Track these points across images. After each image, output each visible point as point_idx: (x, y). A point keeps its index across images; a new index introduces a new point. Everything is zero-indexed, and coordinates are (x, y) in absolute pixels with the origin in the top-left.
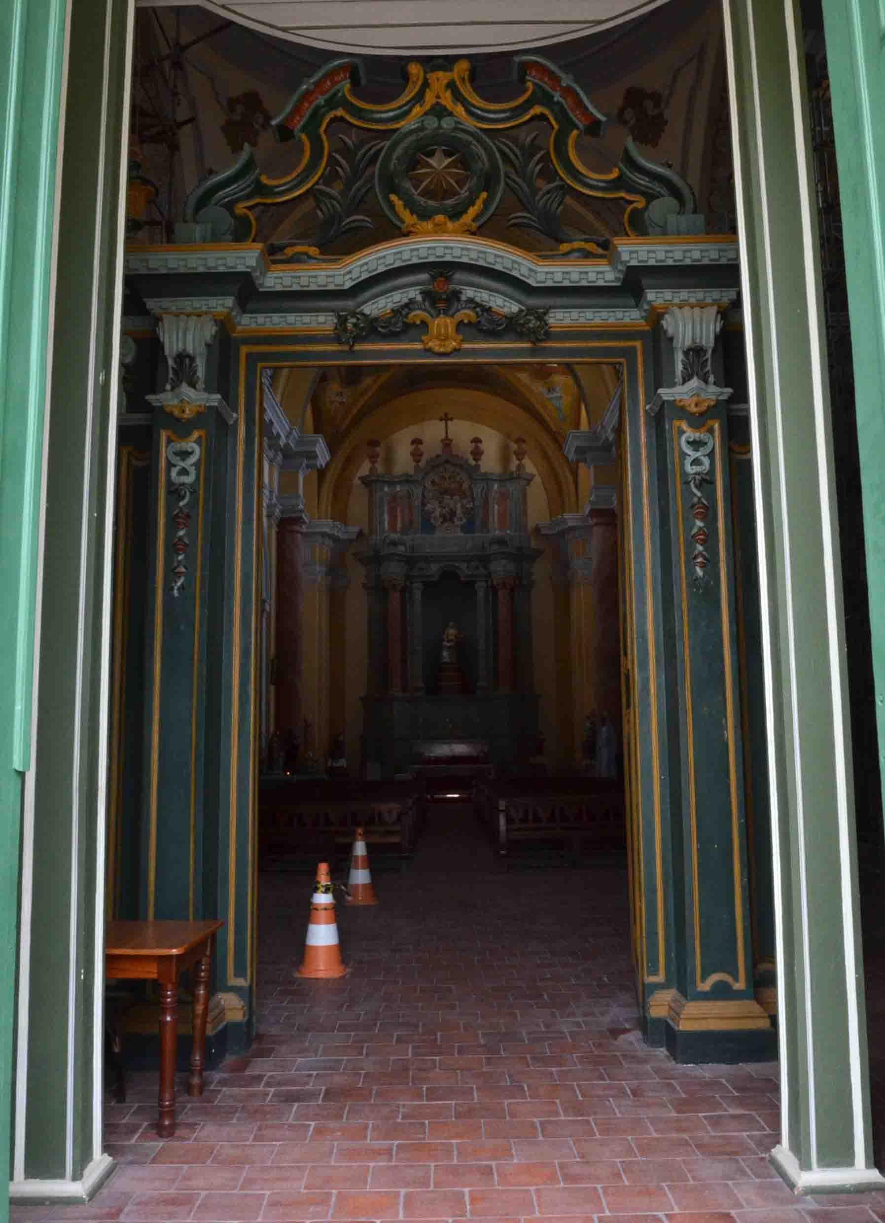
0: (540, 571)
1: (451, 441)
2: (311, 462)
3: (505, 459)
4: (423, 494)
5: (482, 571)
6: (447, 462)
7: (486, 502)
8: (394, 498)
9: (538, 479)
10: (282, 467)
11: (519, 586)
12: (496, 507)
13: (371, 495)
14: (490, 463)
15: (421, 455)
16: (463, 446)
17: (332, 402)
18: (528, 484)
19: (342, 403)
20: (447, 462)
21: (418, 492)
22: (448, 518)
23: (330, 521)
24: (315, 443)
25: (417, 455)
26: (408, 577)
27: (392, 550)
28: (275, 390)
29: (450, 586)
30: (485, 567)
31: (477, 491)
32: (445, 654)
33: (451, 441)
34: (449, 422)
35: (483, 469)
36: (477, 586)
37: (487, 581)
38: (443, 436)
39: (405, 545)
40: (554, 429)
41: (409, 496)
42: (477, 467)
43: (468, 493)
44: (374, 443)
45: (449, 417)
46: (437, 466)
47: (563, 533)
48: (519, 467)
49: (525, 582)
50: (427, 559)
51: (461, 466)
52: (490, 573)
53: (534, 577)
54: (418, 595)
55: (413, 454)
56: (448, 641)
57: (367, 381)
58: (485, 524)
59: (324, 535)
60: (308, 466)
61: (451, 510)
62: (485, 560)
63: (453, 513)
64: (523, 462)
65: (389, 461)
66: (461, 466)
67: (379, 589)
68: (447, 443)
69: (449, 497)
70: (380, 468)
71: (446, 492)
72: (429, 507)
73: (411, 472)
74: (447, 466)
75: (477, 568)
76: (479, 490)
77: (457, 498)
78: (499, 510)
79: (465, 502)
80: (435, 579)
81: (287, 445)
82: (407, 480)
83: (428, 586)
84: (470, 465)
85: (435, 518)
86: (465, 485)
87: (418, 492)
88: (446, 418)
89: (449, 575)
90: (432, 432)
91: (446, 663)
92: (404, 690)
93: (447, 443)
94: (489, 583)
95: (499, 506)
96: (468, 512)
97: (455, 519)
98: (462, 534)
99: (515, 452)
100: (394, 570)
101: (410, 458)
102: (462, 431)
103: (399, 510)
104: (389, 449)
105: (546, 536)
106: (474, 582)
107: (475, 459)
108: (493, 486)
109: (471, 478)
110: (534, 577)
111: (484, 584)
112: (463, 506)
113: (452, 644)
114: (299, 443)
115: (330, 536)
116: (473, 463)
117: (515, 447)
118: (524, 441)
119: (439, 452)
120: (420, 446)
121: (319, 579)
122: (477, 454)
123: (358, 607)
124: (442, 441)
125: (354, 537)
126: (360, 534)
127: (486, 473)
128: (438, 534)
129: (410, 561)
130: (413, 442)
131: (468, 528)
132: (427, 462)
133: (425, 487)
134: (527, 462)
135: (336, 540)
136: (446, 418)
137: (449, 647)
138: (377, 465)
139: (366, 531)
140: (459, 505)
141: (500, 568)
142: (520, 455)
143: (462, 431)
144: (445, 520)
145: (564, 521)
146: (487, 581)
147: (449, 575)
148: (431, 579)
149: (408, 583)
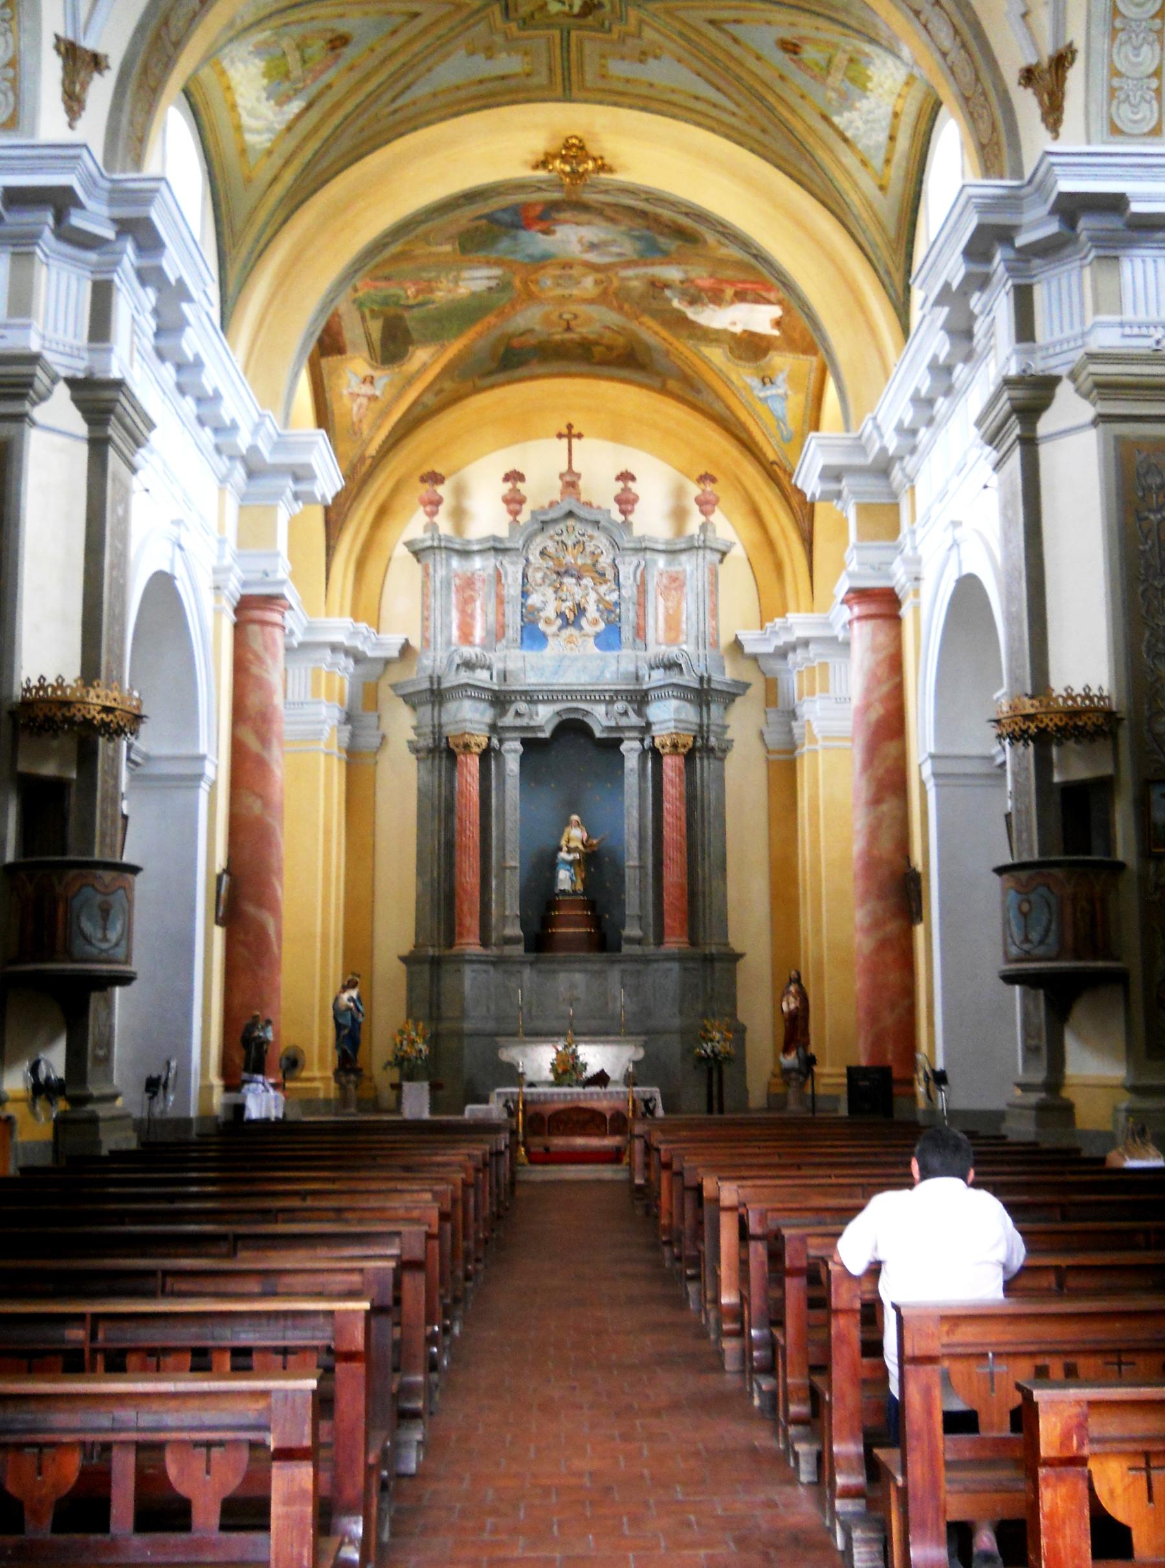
0: (742, 725)
1: (579, 476)
2: (303, 487)
3: (679, 515)
4: (525, 576)
5: (634, 720)
6: (570, 514)
7: (642, 588)
8: (469, 583)
9: (738, 552)
10: (244, 497)
11: (701, 751)
12: (661, 599)
13: (426, 574)
14: (651, 520)
15: (521, 501)
16: (600, 489)
17: (354, 396)
18: (721, 561)
19: (372, 398)
20: (570, 514)
21: (513, 571)
22: (573, 618)
23: (348, 621)
24: (309, 446)
25: (514, 502)
26: (494, 728)
27: (465, 677)
28: (233, 346)
29: (571, 750)
30: (640, 713)
31: (627, 570)
32: (563, 875)
33: (579, 476)
34: (575, 441)
35: (637, 531)
37: (642, 740)
38: (565, 468)
39: (489, 668)
40: (771, 456)
41: (498, 577)
42: (627, 525)
43: (610, 575)
44: (435, 478)
45: (575, 431)
46: (555, 521)
47: (783, 653)
48: (704, 528)
49: (713, 741)
50: (531, 697)
51: (596, 523)
52: (649, 725)
53: (729, 735)
54: (512, 764)
55: (507, 501)
56: (569, 851)
57: (420, 356)
58: (640, 631)
59: (335, 648)
60: (296, 496)
61: (578, 605)
62: (640, 699)
63: (580, 610)
64: (712, 518)
65: (459, 515)
66: (596, 523)
67: (442, 752)
68: (571, 482)
69: (574, 581)
70: (445, 526)
71: (567, 572)
72: (534, 600)
73: (503, 531)
74: (571, 522)
75: (625, 713)
76: (632, 569)
77: (587, 581)
78: (667, 609)
79: (603, 589)
80: (546, 734)
81: (253, 449)
82: (497, 548)
83: (532, 746)
84: (613, 523)
85: (548, 622)
86: (604, 561)
87: (513, 571)
88: (569, 434)
89: (573, 729)
90: (542, 462)
91: (563, 892)
92: (485, 942)
93: (571, 482)
94: (647, 743)
95: (666, 600)
96: (611, 612)
97: (584, 622)
98: (597, 650)
99: (700, 502)
100: (470, 718)
101: (504, 507)
102: (598, 463)
103: (478, 603)
104: (460, 491)
105: (755, 658)
106: (620, 741)
107: (623, 512)
108: (655, 562)
109: (615, 545)
110: (729, 735)
111: (636, 745)
112: (600, 600)
113: (578, 856)
114: (280, 444)
115: (350, 652)
116: (620, 518)
117: (694, 490)
118: (713, 480)
119: (557, 496)
120: (519, 485)
121: (327, 729)
122: (626, 502)
123: (400, 781)
124: (562, 476)
125: (395, 653)
126: (406, 649)
127: (642, 539)
128: (555, 647)
129: (500, 700)
130: (507, 478)
131: (609, 638)
132: (533, 513)
133: (527, 560)
134: (718, 518)
135: (358, 658)
136: (569, 434)
137: (571, 863)
138: (436, 519)
139: (416, 642)
140: (593, 596)
141: (668, 716)
142: (706, 505)
143: (598, 463)
144: (566, 623)
145: (788, 629)
146: (642, 740)
147: (573, 729)
148: (541, 735)
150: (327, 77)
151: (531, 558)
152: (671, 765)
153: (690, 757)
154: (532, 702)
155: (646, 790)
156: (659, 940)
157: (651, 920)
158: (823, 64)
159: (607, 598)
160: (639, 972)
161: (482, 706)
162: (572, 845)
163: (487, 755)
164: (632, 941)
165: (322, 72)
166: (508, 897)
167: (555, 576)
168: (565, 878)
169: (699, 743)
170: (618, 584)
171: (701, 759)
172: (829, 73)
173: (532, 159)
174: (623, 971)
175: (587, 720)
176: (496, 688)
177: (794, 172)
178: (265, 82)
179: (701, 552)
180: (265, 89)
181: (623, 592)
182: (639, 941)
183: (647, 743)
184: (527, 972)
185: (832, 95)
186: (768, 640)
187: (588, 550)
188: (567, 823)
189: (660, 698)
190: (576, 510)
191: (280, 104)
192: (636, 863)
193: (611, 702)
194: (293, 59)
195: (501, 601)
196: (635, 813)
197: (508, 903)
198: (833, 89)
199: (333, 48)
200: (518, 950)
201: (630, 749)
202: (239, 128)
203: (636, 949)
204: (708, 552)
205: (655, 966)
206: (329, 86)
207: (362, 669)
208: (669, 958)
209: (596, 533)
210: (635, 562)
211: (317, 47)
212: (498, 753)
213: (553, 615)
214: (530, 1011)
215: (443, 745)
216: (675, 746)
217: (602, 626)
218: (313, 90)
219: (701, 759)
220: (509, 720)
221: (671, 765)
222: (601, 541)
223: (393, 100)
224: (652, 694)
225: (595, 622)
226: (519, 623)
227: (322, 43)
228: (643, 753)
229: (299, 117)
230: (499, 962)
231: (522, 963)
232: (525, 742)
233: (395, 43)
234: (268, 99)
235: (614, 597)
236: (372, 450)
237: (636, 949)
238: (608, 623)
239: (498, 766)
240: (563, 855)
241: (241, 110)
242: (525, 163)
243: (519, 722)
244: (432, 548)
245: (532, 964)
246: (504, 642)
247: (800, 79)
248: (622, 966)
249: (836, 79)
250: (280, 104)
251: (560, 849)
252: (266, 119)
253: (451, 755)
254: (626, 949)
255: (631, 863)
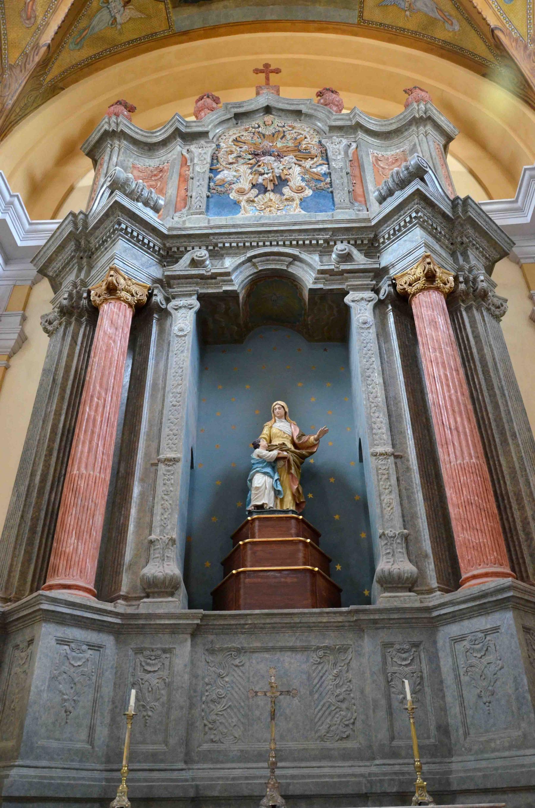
20: (268, 110)
32: (260, 481)
34: (271, 75)
36: (347, 299)
37: (377, 291)
40: (493, 22)
50: (215, 243)
54: (184, 320)
62: (370, 240)
69: (273, 158)
72: (226, 175)
74: (268, 118)
75: (347, 257)
76: (342, 146)
79: (308, 164)
85: (241, 192)
87: (200, 153)
89: (272, 284)
91: (260, 508)
129: (168, 249)
133: (218, 146)
137: (274, 464)
146: (377, 291)
147: (272, 284)
149: (159, 298)
151: (222, 144)
152: (429, 310)
153: (452, 300)
154: (216, 254)
155: (390, 351)
156: (452, 578)
157: (427, 545)
159: (315, 170)
160: (416, 645)
161: (146, 258)
162: (276, 442)
163: (144, 314)
164: (393, 583)
166: (158, 510)
167: (250, 157)
168: (263, 487)
169: (462, 286)
170: (327, 159)
171: (469, 309)
174: (387, 645)
175: (296, 270)
176: (166, 232)
179: (422, 129)
181: (333, 164)
182: (410, 584)
183: (385, 288)
184: (184, 651)
186: (521, 210)
187: (288, 137)
188: (268, 416)
189: (397, 234)
190: (273, 104)
192: (389, 449)
193: (325, 250)
195: (184, 179)
196: (378, 379)
197: (157, 519)
200: (175, 604)
201: (361, 310)
203: (407, 599)
204: (429, 128)
205: (455, 629)
207: (15, 269)
208: (485, 605)
209: (297, 125)
210: (345, 142)
212: (165, 314)
213: (247, 186)
214: (187, 742)
215: (84, 302)
216: (430, 277)
217: (309, 192)
219: (469, 309)
220: (182, 267)
221: (429, 310)
222: (303, 129)
224: (386, 231)
225: (300, 190)
226: (205, 192)
228: (380, 305)
230: (124, 630)
231: (174, 630)
232: (201, 298)
235: (324, 169)
236: (48, 37)
237: (407, 599)
238: (318, 191)
239: (161, 331)
240: (261, 451)
243: (195, 272)
244: (106, 133)
245: (196, 632)
246: (184, 211)
248: (384, 636)
251: (256, 446)
253: (93, 313)
254: (383, 599)
255: (380, 449)
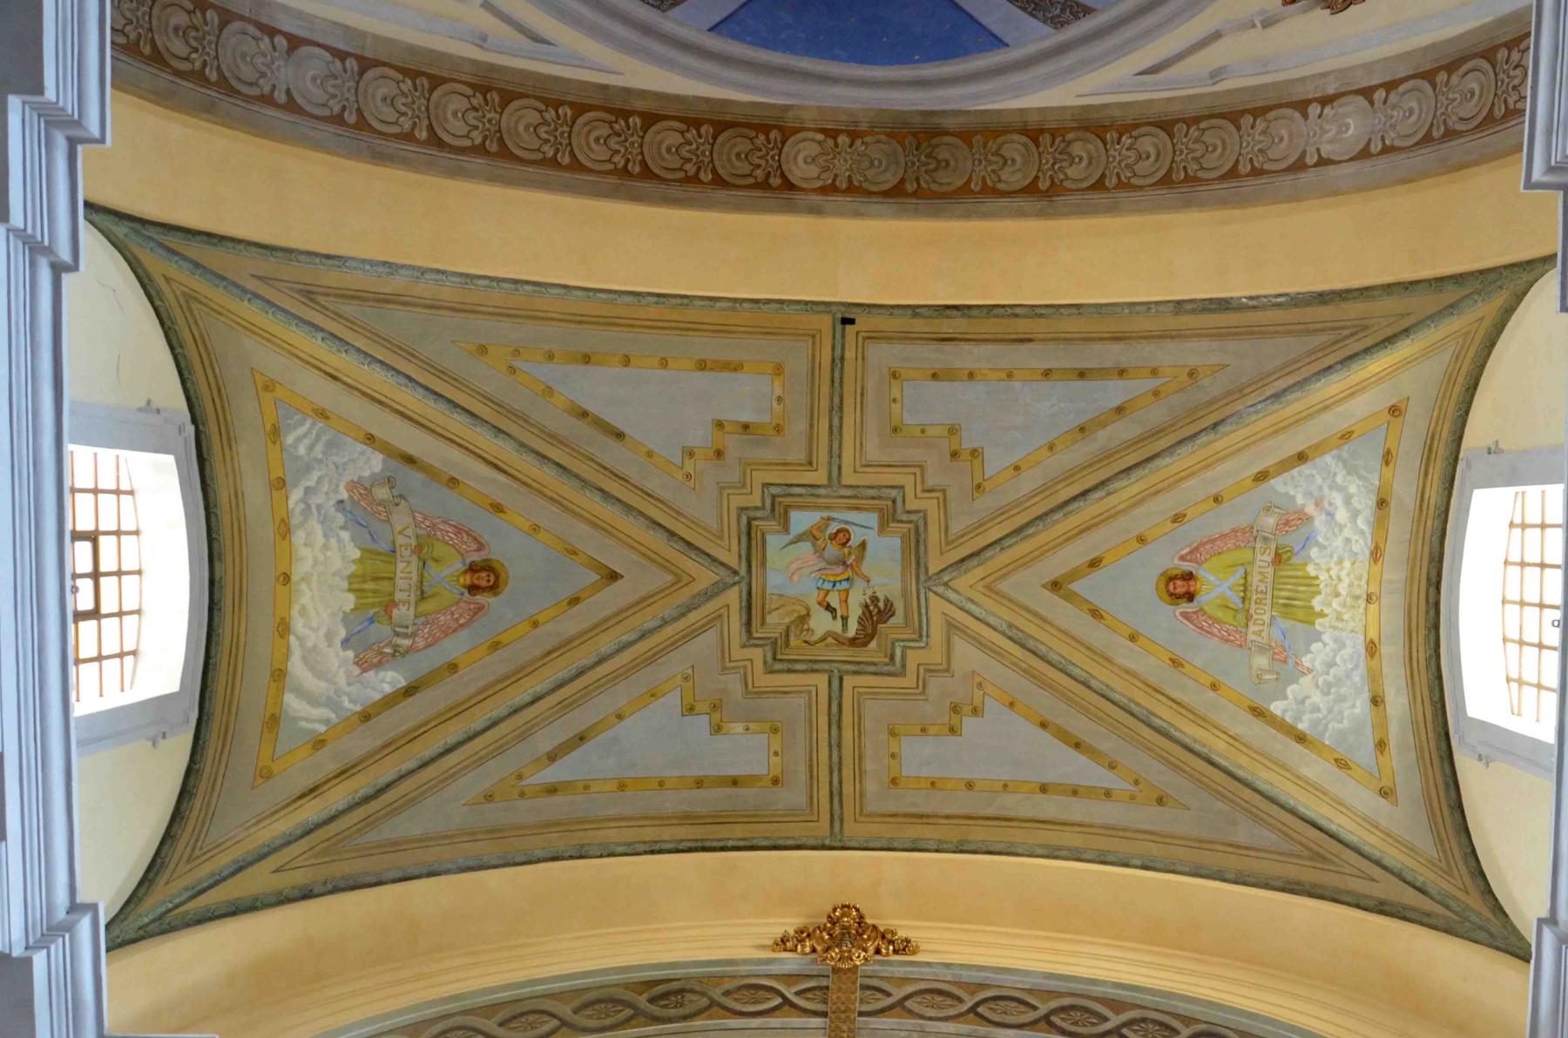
150: (454, 647)
158: (1235, 600)
165: (447, 632)
172: (1248, 618)
173: (770, 942)
177: (1231, 862)
178: (350, 601)
180: (346, 619)
185: (1261, 661)
191: (364, 665)
194: (406, 571)
198: (1262, 649)
199: (473, 589)
202: (280, 675)
206: (453, 667)
211: (449, 570)
218: (427, 661)
223: (552, 757)
227: (459, 566)
229: (390, 701)
233: (572, 623)
234: (346, 643)
241: (292, 638)
242: (763, 947)
247: (1206, 653)
249: (1264, 624)
250: (364, 665)
252: (331, 681)
